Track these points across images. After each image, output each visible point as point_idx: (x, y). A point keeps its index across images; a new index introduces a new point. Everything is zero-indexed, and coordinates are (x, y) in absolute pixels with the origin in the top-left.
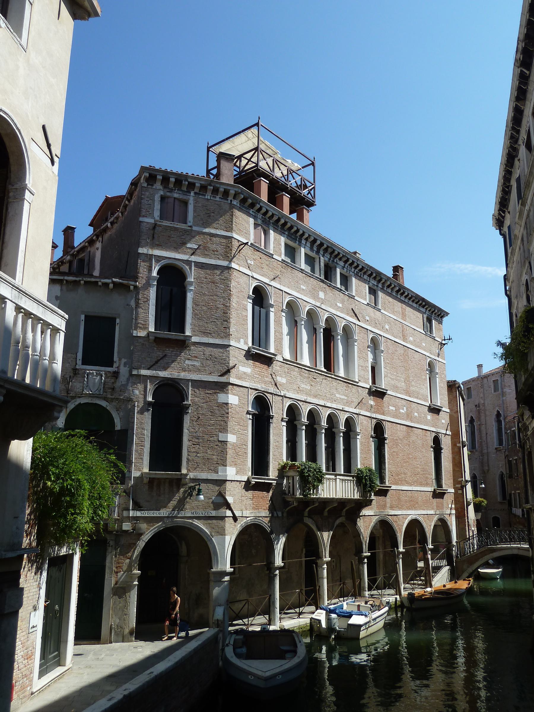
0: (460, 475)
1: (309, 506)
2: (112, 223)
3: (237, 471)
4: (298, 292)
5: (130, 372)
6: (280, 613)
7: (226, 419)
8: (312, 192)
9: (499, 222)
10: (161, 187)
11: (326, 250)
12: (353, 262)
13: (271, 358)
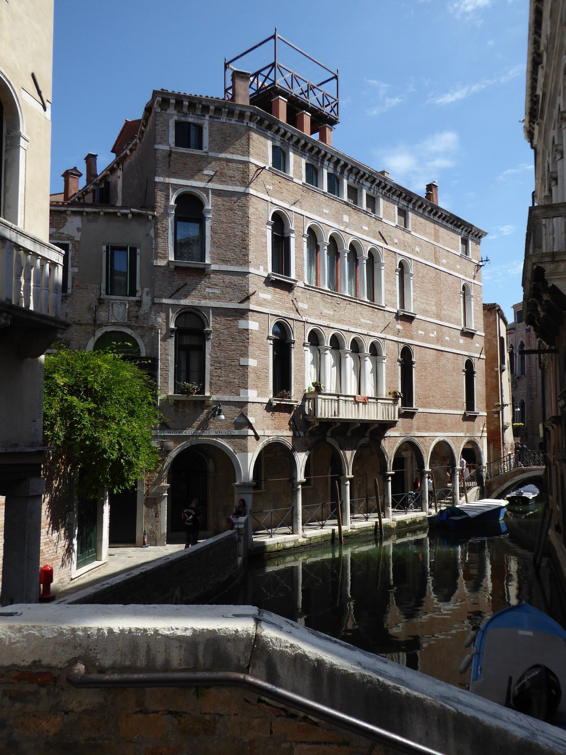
0: (497, 400)
1: (331, 427)
2: (131, 150)
3: (258, 394)
4: (320, 216)
5: (153, 300)
6: (303, 525)
7: (246, 344)
8: (335, 109)
9: (530, 135)
10: (175, 112)
11: (350, 171)
12: (380, 182)
13: (292, 284)
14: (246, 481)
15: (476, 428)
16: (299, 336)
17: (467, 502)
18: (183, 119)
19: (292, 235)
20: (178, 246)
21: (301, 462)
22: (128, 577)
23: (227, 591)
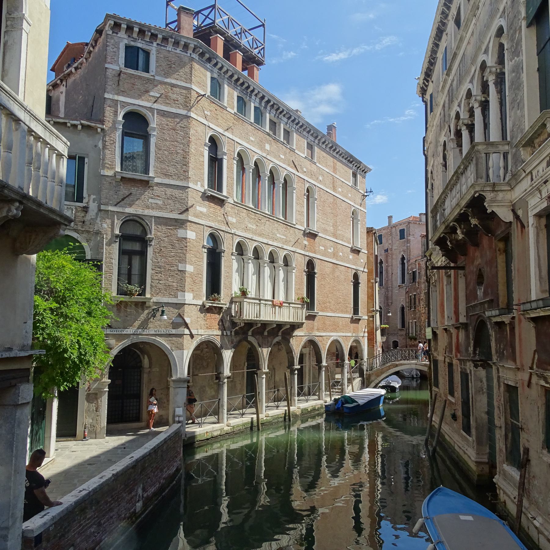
0: (372, 306)
1: (252, 327)
2: (76, 69)
3: (194, 296)
4: (248, 143)
5: (99, 207)
6: (227, 414)
7: (185, 252)
8: (262, 52)
9: (423, 91)
10: (126, 36)
11: (272, 106)
12: (295, 119)
13: (223, 200)
14: (182, 377)
15: (360, 329)
16: (228, 247)
17: (353, 391)
18: (133, 44)
19: (225, 157)
20: (124, 159)
21: (227, 358)
22: (102, 480)
23: (175, 482)
